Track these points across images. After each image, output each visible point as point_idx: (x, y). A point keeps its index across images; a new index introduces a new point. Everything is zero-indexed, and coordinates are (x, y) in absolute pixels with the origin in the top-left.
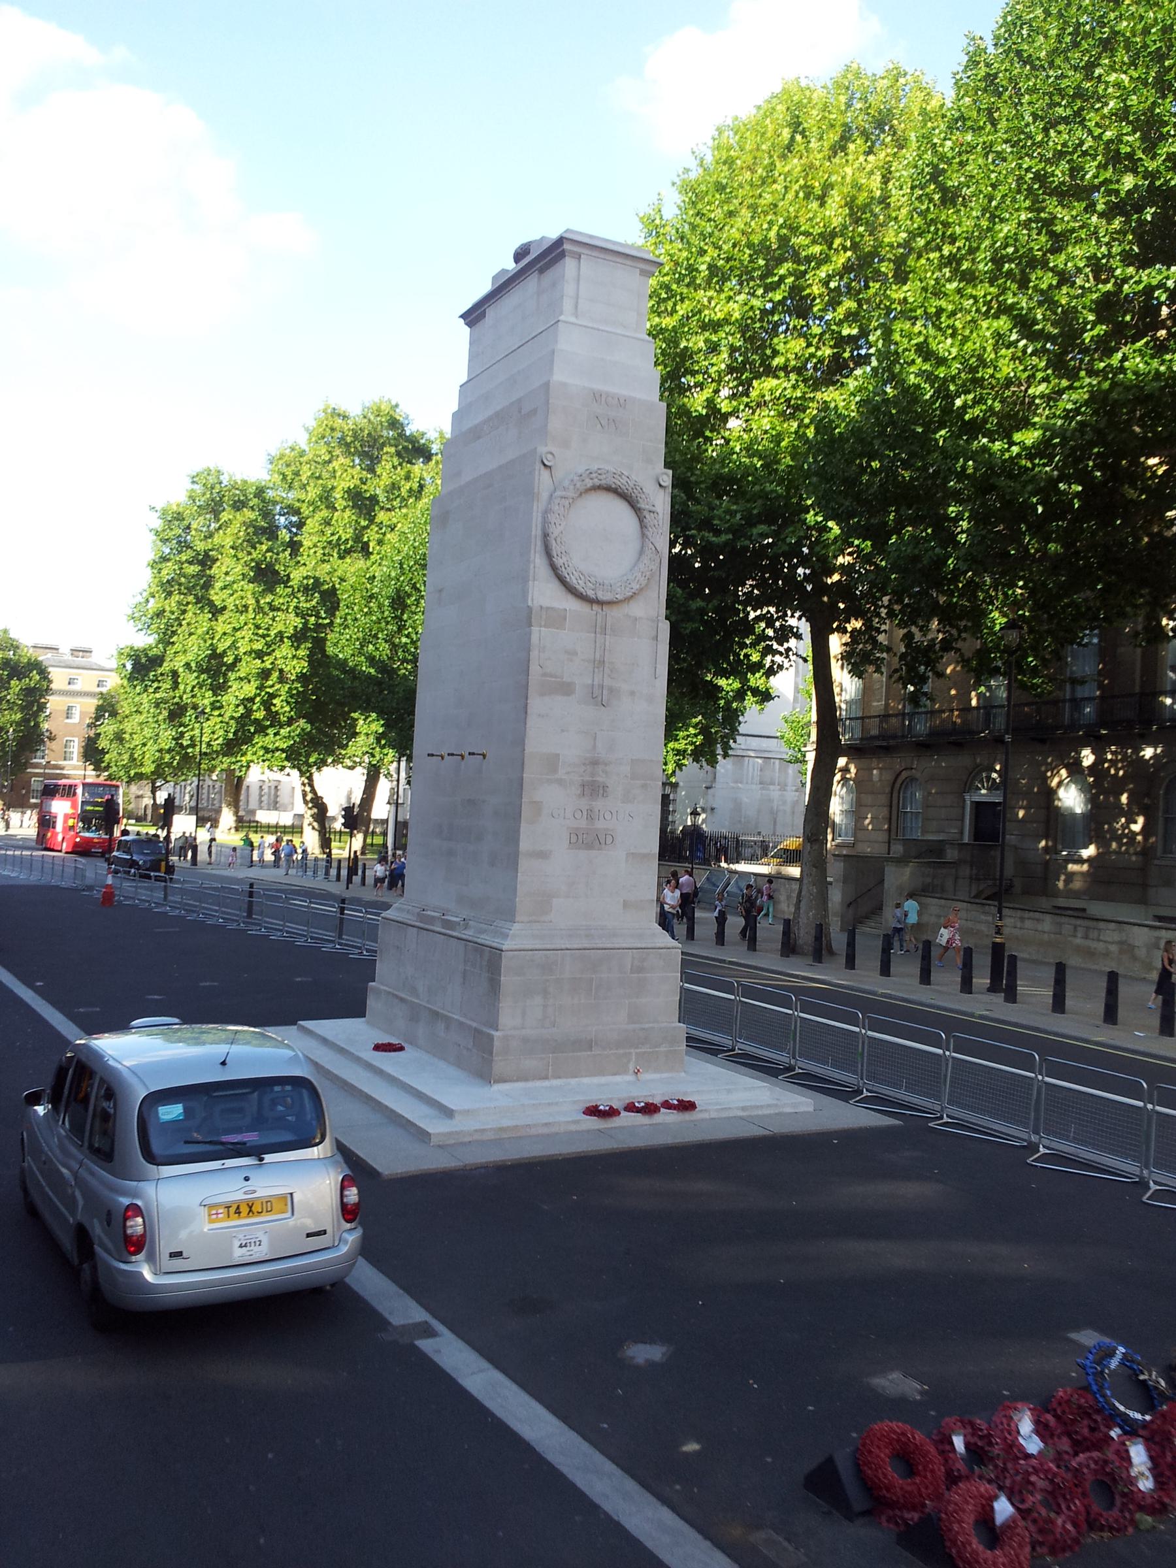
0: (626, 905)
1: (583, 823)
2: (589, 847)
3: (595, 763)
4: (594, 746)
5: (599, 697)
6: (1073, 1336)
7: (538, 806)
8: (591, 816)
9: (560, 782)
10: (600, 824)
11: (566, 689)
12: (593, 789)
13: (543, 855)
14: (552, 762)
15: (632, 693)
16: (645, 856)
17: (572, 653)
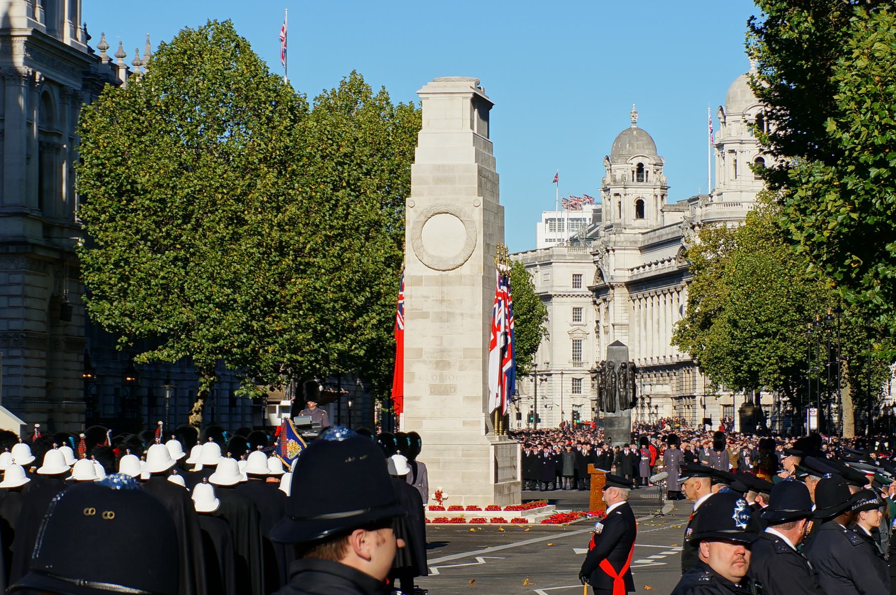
0: (465, 423)
1: (437, 382)
2: (440, 393)
3: (442, 351)
4: (441, 344)
5: (445, 318)
6: (288, 494)
7: (413, 375)
8: (442, 378)
9: (424, 362)
10: (448, 382)
11: (425, 315)
12: (442, 364)
13: (416, 398)
14: (419, 352)
15: (462, 314)
16: (474, 398)
17: (426, 297)
